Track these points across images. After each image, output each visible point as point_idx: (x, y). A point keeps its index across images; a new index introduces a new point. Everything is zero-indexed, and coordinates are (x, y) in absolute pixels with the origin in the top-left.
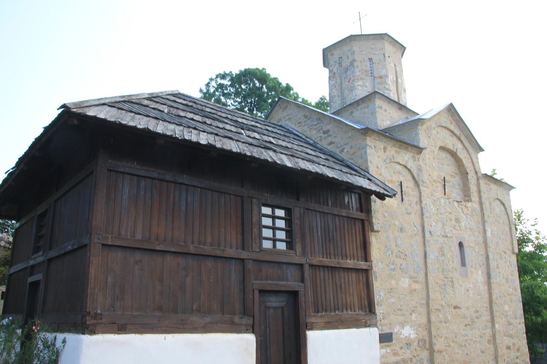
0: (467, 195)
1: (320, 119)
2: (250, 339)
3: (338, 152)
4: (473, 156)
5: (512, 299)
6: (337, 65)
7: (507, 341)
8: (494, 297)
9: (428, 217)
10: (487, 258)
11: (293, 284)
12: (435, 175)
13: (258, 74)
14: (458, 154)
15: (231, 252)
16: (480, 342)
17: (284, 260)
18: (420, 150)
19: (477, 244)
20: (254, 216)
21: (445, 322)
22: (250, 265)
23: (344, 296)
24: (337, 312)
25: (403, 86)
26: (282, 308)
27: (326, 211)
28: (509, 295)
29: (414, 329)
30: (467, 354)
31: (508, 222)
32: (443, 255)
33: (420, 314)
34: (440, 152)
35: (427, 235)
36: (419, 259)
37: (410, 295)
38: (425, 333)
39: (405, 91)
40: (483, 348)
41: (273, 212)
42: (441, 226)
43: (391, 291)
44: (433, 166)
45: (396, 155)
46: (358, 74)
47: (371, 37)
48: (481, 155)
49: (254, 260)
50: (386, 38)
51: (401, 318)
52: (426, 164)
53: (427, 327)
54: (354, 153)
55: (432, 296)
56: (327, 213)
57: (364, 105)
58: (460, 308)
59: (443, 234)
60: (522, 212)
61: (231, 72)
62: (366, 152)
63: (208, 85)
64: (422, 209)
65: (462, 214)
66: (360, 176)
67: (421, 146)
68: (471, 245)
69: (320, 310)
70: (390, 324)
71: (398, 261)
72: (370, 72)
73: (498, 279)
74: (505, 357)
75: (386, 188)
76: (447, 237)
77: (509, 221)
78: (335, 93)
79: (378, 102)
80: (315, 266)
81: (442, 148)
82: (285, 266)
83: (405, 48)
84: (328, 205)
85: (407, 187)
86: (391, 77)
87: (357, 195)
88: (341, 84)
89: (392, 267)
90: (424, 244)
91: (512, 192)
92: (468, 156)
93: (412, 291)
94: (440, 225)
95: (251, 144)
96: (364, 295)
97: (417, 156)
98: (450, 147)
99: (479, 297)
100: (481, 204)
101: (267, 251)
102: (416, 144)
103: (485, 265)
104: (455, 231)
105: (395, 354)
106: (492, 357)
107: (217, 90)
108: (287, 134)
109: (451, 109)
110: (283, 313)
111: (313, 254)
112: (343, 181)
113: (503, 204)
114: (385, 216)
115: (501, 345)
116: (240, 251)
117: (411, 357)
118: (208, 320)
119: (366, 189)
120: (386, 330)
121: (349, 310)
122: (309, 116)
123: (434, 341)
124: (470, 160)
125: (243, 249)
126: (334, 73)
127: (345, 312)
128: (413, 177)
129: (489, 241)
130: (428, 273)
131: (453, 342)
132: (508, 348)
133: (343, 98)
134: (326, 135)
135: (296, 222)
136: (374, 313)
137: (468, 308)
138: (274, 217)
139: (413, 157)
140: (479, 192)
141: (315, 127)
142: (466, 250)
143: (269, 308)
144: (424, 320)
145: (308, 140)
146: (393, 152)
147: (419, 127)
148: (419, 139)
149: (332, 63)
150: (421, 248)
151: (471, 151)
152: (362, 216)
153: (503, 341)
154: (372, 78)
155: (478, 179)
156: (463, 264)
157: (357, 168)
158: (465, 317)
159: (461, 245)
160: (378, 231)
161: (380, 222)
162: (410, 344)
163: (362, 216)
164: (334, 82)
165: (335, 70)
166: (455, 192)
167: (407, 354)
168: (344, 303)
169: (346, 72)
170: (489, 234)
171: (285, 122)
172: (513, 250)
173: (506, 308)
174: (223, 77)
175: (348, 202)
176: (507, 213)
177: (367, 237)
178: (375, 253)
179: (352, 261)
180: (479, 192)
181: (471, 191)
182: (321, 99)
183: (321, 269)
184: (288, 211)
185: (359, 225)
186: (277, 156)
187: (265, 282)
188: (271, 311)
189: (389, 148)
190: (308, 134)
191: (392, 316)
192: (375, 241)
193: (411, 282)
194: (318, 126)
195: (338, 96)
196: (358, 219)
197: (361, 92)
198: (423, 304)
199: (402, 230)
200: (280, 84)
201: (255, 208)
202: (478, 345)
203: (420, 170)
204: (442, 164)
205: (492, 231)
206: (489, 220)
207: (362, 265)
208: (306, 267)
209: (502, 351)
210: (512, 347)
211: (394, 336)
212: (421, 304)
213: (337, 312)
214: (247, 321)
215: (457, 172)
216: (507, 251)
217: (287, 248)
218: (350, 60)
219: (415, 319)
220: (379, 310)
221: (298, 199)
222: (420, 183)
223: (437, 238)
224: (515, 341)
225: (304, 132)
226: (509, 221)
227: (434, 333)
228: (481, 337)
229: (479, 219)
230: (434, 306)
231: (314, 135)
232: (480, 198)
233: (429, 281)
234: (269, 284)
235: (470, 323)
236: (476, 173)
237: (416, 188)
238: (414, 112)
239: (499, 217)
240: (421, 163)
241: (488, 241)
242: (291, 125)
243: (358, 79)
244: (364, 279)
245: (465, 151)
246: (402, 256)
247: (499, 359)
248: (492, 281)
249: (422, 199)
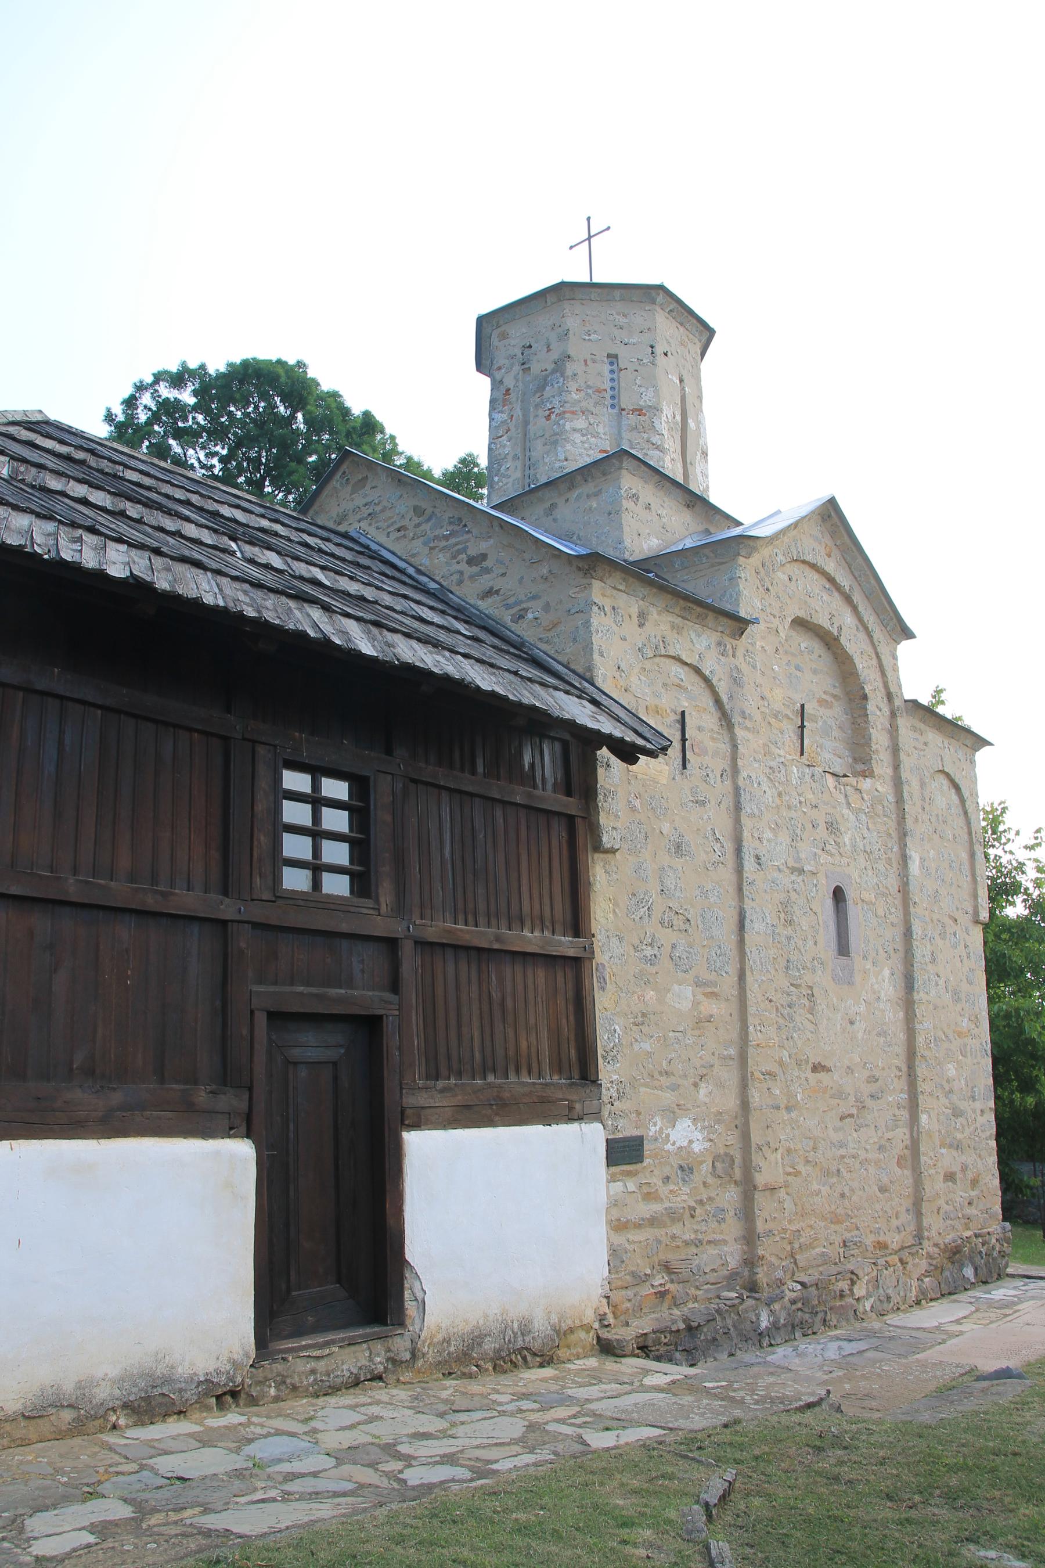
0: (861, 760)
1: (460, 519)
2: (240, 1153)
3: (507, 619)
4: (884, 650)
5: (965, 1045)
6: (517, 368)
7: (949, 1159)
8: (920, 1040)
9: (752, 815)
10: (908, 933)
11: (365, 995)
12: (778, 697)
13: (283, 379)
14: (843, 641)
15: (188, 900)
16: (877, 1162)
17: (344, 927)
18: (739, 624)
19: (883, 894)
20: (259, 796)
21: (788, 1109)
22: (244, 941)
23: (511, 1032)
24: (491, 1078)
25: (701, 442)
26: (335, 1064)
27: (469, 789)
28: (960, 1035)
29: (704, 1128)
30: (843, 1195)
31: (966, 837)
32: (790, 922)
33: (721, 1085)
34: (794, 634)
35: (749, 864)
36: (725, 933)
37: (697, 1032)
38: (733, 1138)
39: (705, 454)
40: (885, 1180)
41: (316, 786)
42: (789, 841)
43: (642, 1020)
44: (775, 673)
45: (671, 636)
46: (575, 396)
47: (617, 293)
48: (904, 648)
49: (255, 925)
50: (661, 298)
51: (668, 1098)
52: (754, 667)
53: (737, 1122)
54: (555, 625)
55: (754, 1036)
56: (472, 795)
57: (589, 488)
59: (791, 863)
60: (1004, 810)
61: (203, 367)
62: (587, 624)
63: (130, 403)
64: (737, 791)
65: (846, 811)
66: (567, 692)
67: (742, 614)
68: (865, 895)
69: (444, 1071)
70: (639, 1113)
71: (666, 937)
72: (610, 393)
73: (933, 993)
74: (941, 1202)
75: (640, 729)
76: (801, 871)
77: (970, 834)
78: (507, 447)
79: (629, 482)
80: (432, 944)
81: (800, 623)
82: (345, 944)
83: (711, 332)
84: (473, 772)
85: (700, 729)
86: (669, 412)
87: (558, 746)
88: (526, 423)
89: (649, 952)
90: (740, 889)
91: (982, 756)
92: (870, 650)
93: (702, 1022)
94: (784, 838)
95: (258, 585)
96: (567, 1029)
97: (729, 642)
98: (822, 620)
99: (882, 1039)
100: (898, 783)
101: (294, 897)
102: (728, 607)
103: (901, 954)
104: (824, 858)
105: (650, 1196)
106: (908, 1203)
107: (155, 418)
108: (364, 561)
109: (830, 515)
110: (336, 1078)
111: (428, 912)
112: (520, 704)
113: (957, 788)
114: (633, 809)
115: (932, 1171)
116: (214, 896)
117: (693, 1204)
118: (117, 1098)
119: (584, 729)
120: (627, 1130)
121: (524, 1072)
122: (428, 512)
123: (756, 1159)
124: (875, 662)
125: (225, 893)
126: (508, 390)
127: (513, 1078)
128: (718, 702)
129: (913, 886)
130: (748, 973)
132: (950, 1177)
133: (529, 465)
134: (475, 569)
135: (381, 817)
136: (595, 1082)
137: (850, 1070)
138: (317, 801)
139: (719, 644)
140: (895, 750)
141: (444, 543)
142: (853, 910)
143: (295, 1064)
144: (731, 1102)
145: (423, 579)
146: (664, 628)
147: (741, 560)
148: (739, 593)
149: (501, 360)
150: (732, 902)
151: (878, 635)
152: (571, 805)
153: (938, 1159)
154: (616, 411)
155: (893, 715)
156: (843, 948)
157: (560, 668)
158: (840, 1094)
159: (838, 895)
160: (613, 851)
161: (618, 825)
162: (691, 1169)
163: (571, 805)
164: (505, 416)
165: (509, 382)
166: (828, 748)
167: (682, 1196)
168: (511, 1053)
169: (541, 388)
170: (914, 867)
171: (357, 525)
172: (976, 913)
173: (951, 1070)
174: (177, 380)
175: (532, 765)
176: (966, 813)
177: (581, 867)
178: (604, 911)
179: (537, 934)
180: (895, 750)
181: (874, 747)
182: (463, 461)
183: (450, 953)
184: (360, 785)
185: (559, 832)
186: (333, 623)
187: (287, 989)
188: (303, 1073)
189: (654, 614)
190: (424, 561)
191: (642, 1089)
192: (605, 882)
193: (701, 997)
194: (453, 541)
195: (516, 457)
196: (559, 814)
197: (581, 449)
199: (678, 848)
200: (346, 412)
201: (263, 770)
202: (872, 1170)
203: (736, 681)
204: (798, 668)
205: (922, 860)
206: (918, 829)
207: (566, 944)
208: (407, 950)
209: (935, 1185)
210: (959, 1176)
211: (647, 1146)
212: (725, 1058)
213: (491, 1078)
214: (233, 1101)
215: (837, 691)
216: (958, 915)
217: (352, 892)
218: (554, 355)
219: (707, 1100)
220: (608, 1073)
221: (389, 752)
222: (736, 719)
223: (776, 874)
224: (969, 1158)
225: (414, 556)
226: (970, 834)
227: (756, 1138)
228: (881, 1148)
229: (892, 824)
230: (758, 1063)
231: (440, 566)
232: (896, 767)
233: (748, 992)
234: (300, 995)
235: (854, 1111)
236: (890, 697)
237: (725, 732)
238: (728, 517)
239: (945, 822)
240: (740, 661)
241: (911, 888)
242: (376, 535)
243: (573, 413)
244: (570, 985)
245: (862, 635)
246: (678, 922)
247: (925, 1208)
248: (916, 997)
249: (740, 763)
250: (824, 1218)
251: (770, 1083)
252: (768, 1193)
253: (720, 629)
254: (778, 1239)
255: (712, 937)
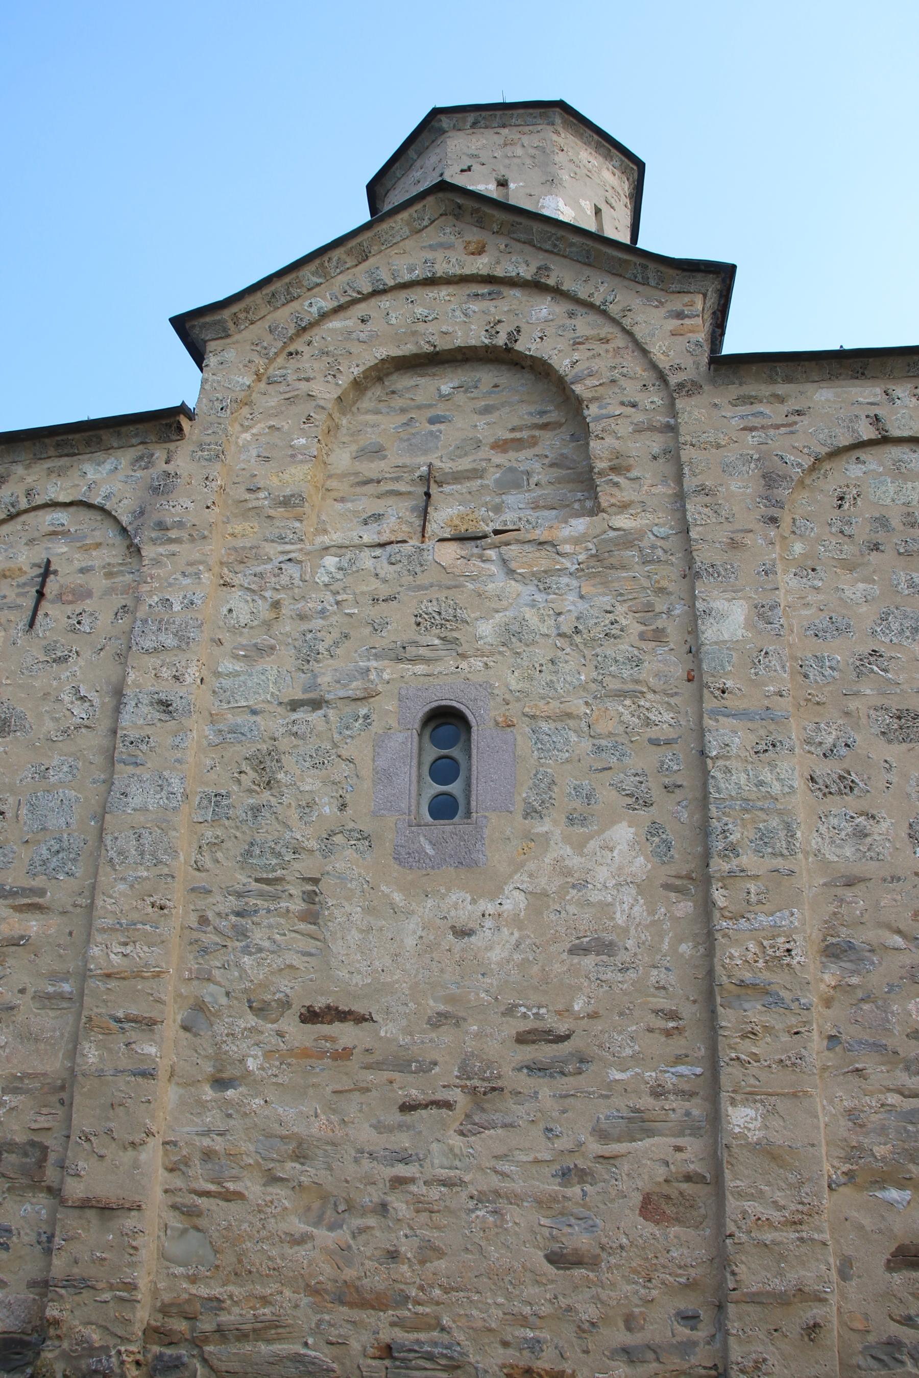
58: (361, 1019)
131: (273, 1180)
198: (61, 996)
250: (314, 1291)
251: (133, 1035)
252: (91, 1214)
253: (134, 441)
254: (107, 1296)
255: (44, 829)
